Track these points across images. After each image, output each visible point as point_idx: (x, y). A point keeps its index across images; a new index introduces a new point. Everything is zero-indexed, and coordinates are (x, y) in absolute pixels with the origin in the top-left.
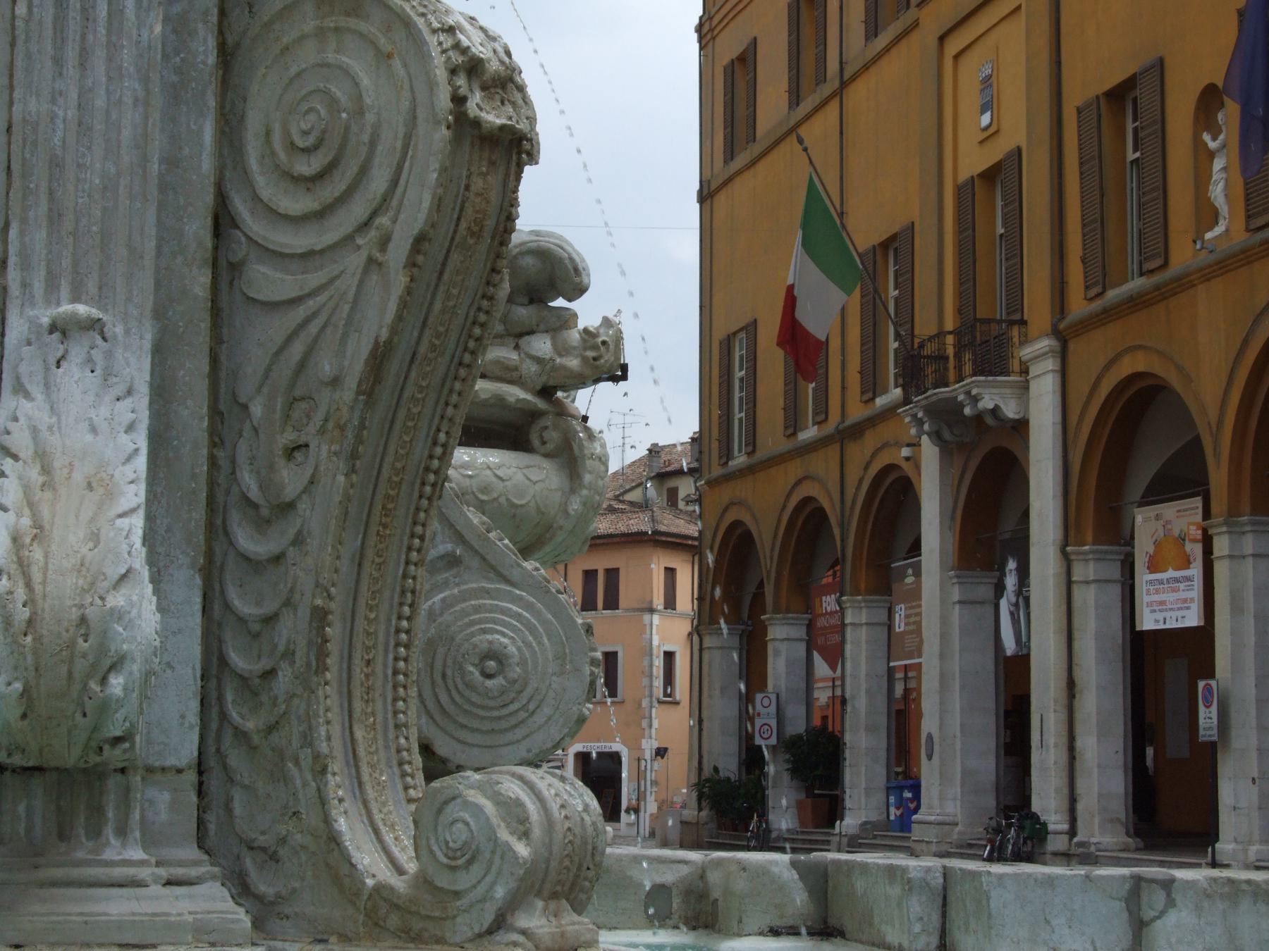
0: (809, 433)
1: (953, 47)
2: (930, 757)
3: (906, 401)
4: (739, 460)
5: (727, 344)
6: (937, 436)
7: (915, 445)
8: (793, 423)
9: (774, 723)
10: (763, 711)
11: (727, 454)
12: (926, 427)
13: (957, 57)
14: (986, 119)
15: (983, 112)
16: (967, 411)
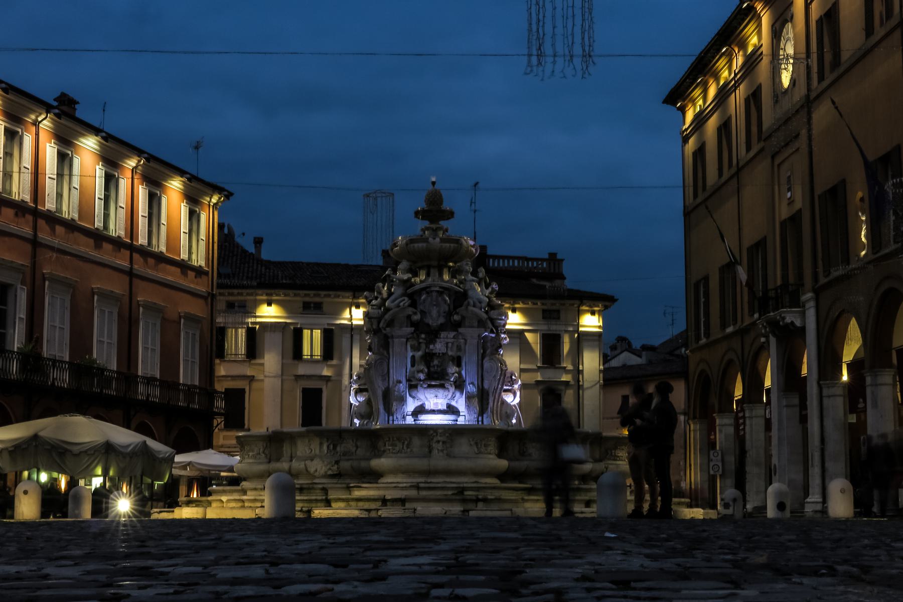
0: (730, 330)
1: (777, 162)
2: (775, 474)
3: (759, 319)
4: (704, 341)
5: (697, 285)
6: (775, 335)
7: (767, 337)
8: (724, 326)
9: (720, 464)
10: (714, 458)
11: (698, 338)
12: (768, 329)
13: (779, 165)
14: (789, 195)
15: (788, 192)
16: (781, 323)
